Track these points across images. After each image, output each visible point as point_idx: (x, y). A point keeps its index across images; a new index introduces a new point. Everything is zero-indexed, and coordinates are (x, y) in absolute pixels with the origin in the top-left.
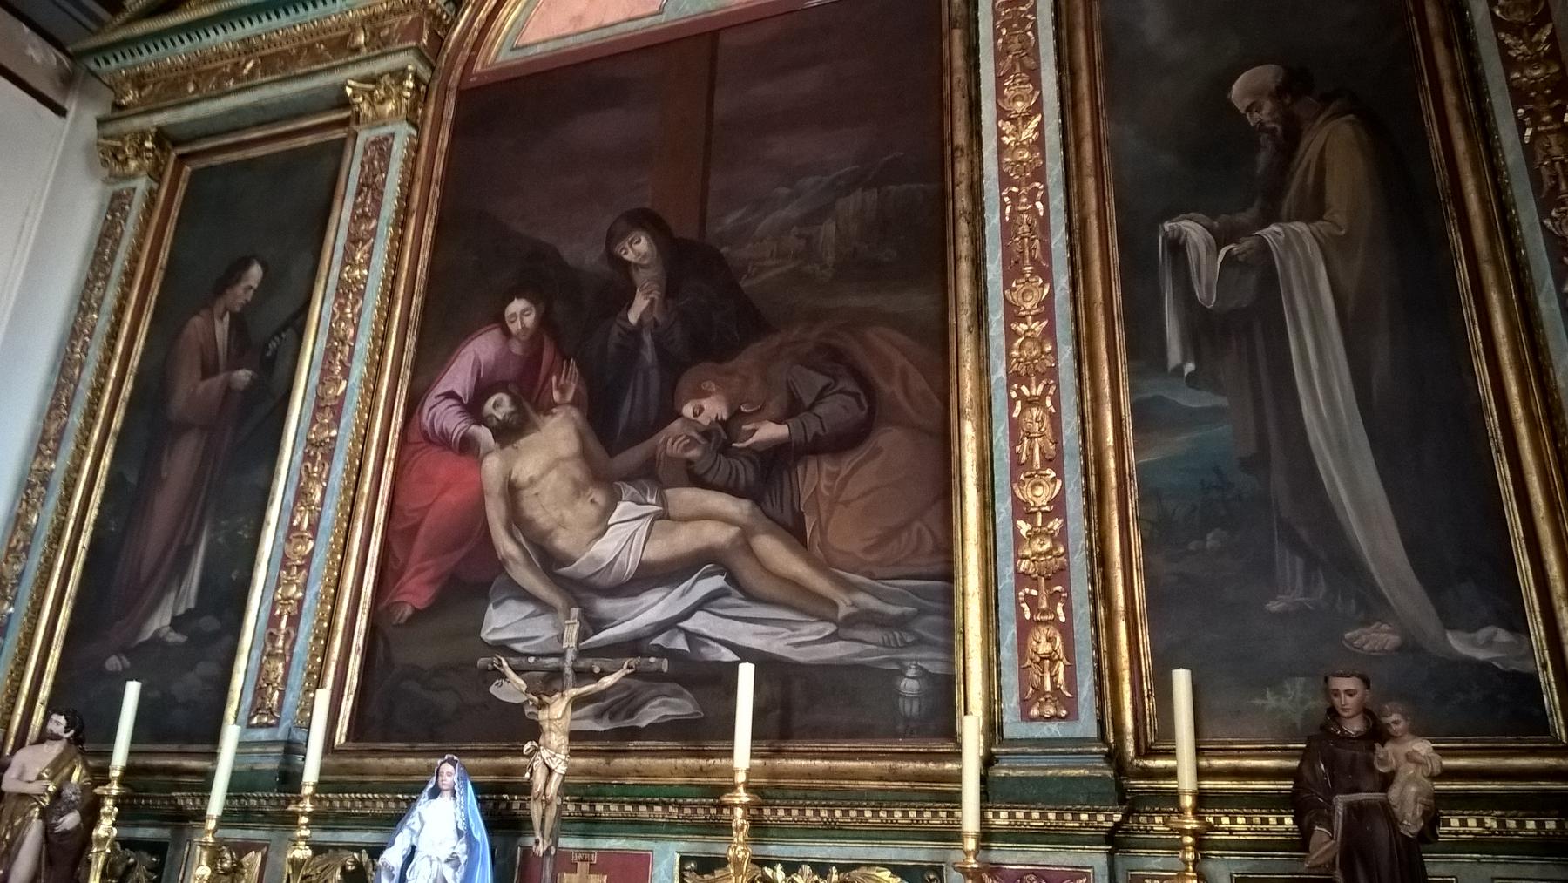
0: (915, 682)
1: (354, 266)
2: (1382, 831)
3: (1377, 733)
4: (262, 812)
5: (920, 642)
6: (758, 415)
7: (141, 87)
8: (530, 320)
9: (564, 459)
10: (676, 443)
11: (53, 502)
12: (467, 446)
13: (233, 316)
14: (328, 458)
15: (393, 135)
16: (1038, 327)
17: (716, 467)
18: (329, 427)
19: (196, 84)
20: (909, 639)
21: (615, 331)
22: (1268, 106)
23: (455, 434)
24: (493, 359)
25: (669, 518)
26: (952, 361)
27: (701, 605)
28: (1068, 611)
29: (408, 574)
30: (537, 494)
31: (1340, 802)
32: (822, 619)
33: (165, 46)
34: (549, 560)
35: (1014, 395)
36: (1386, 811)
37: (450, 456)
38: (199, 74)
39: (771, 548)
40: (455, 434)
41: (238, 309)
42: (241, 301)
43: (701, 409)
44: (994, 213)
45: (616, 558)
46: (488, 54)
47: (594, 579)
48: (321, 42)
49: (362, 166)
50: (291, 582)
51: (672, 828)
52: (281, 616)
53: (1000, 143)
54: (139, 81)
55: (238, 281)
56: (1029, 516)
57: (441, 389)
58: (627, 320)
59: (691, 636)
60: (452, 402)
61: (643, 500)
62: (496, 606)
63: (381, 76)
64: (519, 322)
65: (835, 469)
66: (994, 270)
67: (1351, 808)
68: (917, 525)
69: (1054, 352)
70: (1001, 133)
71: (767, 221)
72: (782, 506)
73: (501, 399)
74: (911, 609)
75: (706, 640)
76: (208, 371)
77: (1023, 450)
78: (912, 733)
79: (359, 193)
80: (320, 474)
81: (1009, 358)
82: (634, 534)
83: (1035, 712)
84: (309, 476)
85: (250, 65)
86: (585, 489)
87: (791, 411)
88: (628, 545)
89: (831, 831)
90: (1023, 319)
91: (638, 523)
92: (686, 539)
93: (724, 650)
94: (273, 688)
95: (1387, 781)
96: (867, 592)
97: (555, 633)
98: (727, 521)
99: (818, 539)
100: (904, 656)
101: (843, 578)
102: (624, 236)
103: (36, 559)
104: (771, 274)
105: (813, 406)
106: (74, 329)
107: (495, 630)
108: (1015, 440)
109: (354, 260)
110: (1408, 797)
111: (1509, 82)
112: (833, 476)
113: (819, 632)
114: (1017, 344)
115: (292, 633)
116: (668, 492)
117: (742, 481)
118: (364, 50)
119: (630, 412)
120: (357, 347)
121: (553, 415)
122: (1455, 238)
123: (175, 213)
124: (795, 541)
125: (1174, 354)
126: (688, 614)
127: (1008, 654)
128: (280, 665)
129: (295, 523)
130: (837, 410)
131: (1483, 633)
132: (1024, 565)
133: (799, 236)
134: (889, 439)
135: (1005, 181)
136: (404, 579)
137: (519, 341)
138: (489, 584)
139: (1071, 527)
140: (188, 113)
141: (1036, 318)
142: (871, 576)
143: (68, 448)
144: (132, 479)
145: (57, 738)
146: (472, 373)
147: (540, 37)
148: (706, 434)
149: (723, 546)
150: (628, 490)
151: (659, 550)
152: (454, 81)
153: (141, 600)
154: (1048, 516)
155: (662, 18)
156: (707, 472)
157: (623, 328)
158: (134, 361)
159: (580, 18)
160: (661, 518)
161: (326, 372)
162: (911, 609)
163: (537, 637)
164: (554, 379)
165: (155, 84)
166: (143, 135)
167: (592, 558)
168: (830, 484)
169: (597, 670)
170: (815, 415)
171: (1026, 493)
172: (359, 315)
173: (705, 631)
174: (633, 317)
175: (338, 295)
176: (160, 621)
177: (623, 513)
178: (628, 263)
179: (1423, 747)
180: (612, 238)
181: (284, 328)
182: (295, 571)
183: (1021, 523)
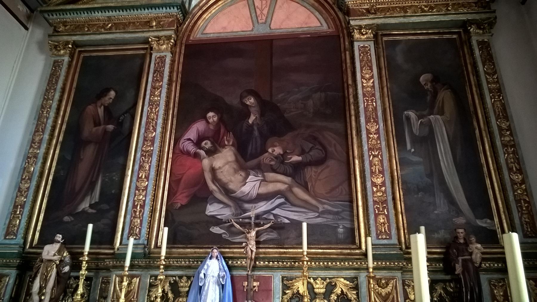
0: (342, 230)
1: (155, 96)
2: (470, 265)
4: (138, 266)
5: (343, 219)
6: (292, 153)
7: (65, 26)
8: (216, 119)
9: (230, 162)
10: (267, 160)
11: (39, 164)
12: (196, 155)
13: (105, 107)
14: (151, 156)
15: (166, 56)
16: (376, 136)
17: (280, 167)
18: (150, 146)
19: (87, 28)
20: (340, 218)
21: (245, 125)
22: (429, 84)
23: (192, 152)
24: (203, 129)
25: (266, 181)
26: (350, 143)
27: (277, 207)
28: (388, 211)
29: (178, 194)
30: (222, 172)
31: (460, 259)
32: (315, 211)
33: (77, 14)
34: (227, 192)
35: (370, 154)
36: (471, 260)
37: (191, 158)
38: (89, 25)
39: (298, 191)
40: (192, 152)
41: (106, 105)
42: (108, 102)
43: (274, 151)
44: (362, 104)
45: (249, 192)
46: (194, 35)
47: (243, 198)
48: (137, 22)
49: (155, 64)
50: (140, 195)
51: (279, 268)
52: (137, 205)
53: (362, 85)
54: (65, 24)
55: (106, 96)
56: (376, 186)
57: (186, 137)
58: (249, 122)
59: (275, 215)
60: (190, 142)
61: (257, 175)
62: (210, 205)
63: (162, 37)
64: (212, 119)
65: (316, 170)
66: (363, 120)
67: (463, 260)
68: (340, 187)
69: (380, 143)
70: (362, 83)
71: (292, 98)
72: (301, 179)
73: (207, 142)
74: (340, 210)
75: (281, 217)
76: (97, 124)
77: (373, 168)
78: (342, 243)
79: (154, 73)
80: (148, 161)
81: (368, 144)
82: (255, 185)
83: (380, 237)
84: (144, 161)
85: (110, 25)
86: (238, 171)
87: (302, 153)
88: (253, 188)
89: (327, 268)
90: (371, 134)
91: (257, 182)
92: (271, 188)
93: (285, 219)
94: (137, 228)
95: (471, 254)
96: (327, 204)
97: (231, 213)
98: (285, 183)
99: (312, 189)
100: (339, 222)
101: (320, 200)
102: (246, 97)
103: (34, 183)
104: (294, 113)
105: (308, 152)
106: (42, 105)
107: (210, 212)
108: (371, 166)
109: (155, 94)
111: (488, 87)
112: (315, 172)
113: (314, 215)
114: (370, 140)
115: (143, 211)
116: (265, 174)
117: (288, 172)
118: (155, 27)
119: (252, 150)
120: (158, 122)
121: (226, 148)
122: (475, 124)
123: (78, 70)
124: (305, 189)
125: (409, 146)
126: (274, 209)
127: (372, 222)
128: (139, 221)
129: (140, 176)
130: (315, 154)
131: (484, 220)
132: (375, 199)
133: (302, 103)
134: (331, 163)
135: (364, 95)
136: (177, 195)
137: (212, 125)
138: (207, 198)
139: (387, 189)
140: (86, 38)
141: (375, 134)
142: (328, 200)
143: (44, 146)
144: (69, 157)
145: (59, 242)
146: (197, 134)
147: (211, 32)
148: (276, 157)
149: (284, 190)
150: (252, 172)
151: (263, 190)
152: (184, 42)
154: (381, 187)
155: (253, 33)
156: (277, 169)
157: (247, 124)
158: (66, 119)
159: (225, 28)
160: (263, 181)
161: (147, 129)
162: (340, 210)
163: (225, 214)
164: (225, 137)
165: (71, 25)
166: (67, 43)
167: (241, 192)
168: (315, 174)
169: (262, 223)
170: (310, 155)
171: (375, 180)
172: (158, 111)
173: (279, 214)
174: (250, 121)
175: (149, 105)
177: (250, 179)
178: (247, 105)
179: (479, 246)
180: (242, 97)
181: (126, 112)
182: (141, 191)
183: (374, 188)
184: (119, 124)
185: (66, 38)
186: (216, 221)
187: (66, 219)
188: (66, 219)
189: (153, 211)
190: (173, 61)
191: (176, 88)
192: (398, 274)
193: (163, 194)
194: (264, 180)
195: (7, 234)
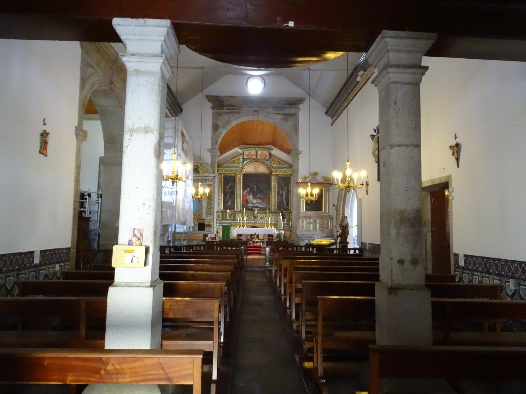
3: (283, 211)
34: (252, 202)
39: (262, 202)
92: (258, 202)
103: (221, 200)
110: (284, 213)
153: (228, 202)
161: (238, 191)
176: (229, 204)
184: (233, 190)
185: (221, 173)
186: (249, 206)
189: (240, 205)
191: (242, 184)
192: (275, 215)
193: (242, 202)
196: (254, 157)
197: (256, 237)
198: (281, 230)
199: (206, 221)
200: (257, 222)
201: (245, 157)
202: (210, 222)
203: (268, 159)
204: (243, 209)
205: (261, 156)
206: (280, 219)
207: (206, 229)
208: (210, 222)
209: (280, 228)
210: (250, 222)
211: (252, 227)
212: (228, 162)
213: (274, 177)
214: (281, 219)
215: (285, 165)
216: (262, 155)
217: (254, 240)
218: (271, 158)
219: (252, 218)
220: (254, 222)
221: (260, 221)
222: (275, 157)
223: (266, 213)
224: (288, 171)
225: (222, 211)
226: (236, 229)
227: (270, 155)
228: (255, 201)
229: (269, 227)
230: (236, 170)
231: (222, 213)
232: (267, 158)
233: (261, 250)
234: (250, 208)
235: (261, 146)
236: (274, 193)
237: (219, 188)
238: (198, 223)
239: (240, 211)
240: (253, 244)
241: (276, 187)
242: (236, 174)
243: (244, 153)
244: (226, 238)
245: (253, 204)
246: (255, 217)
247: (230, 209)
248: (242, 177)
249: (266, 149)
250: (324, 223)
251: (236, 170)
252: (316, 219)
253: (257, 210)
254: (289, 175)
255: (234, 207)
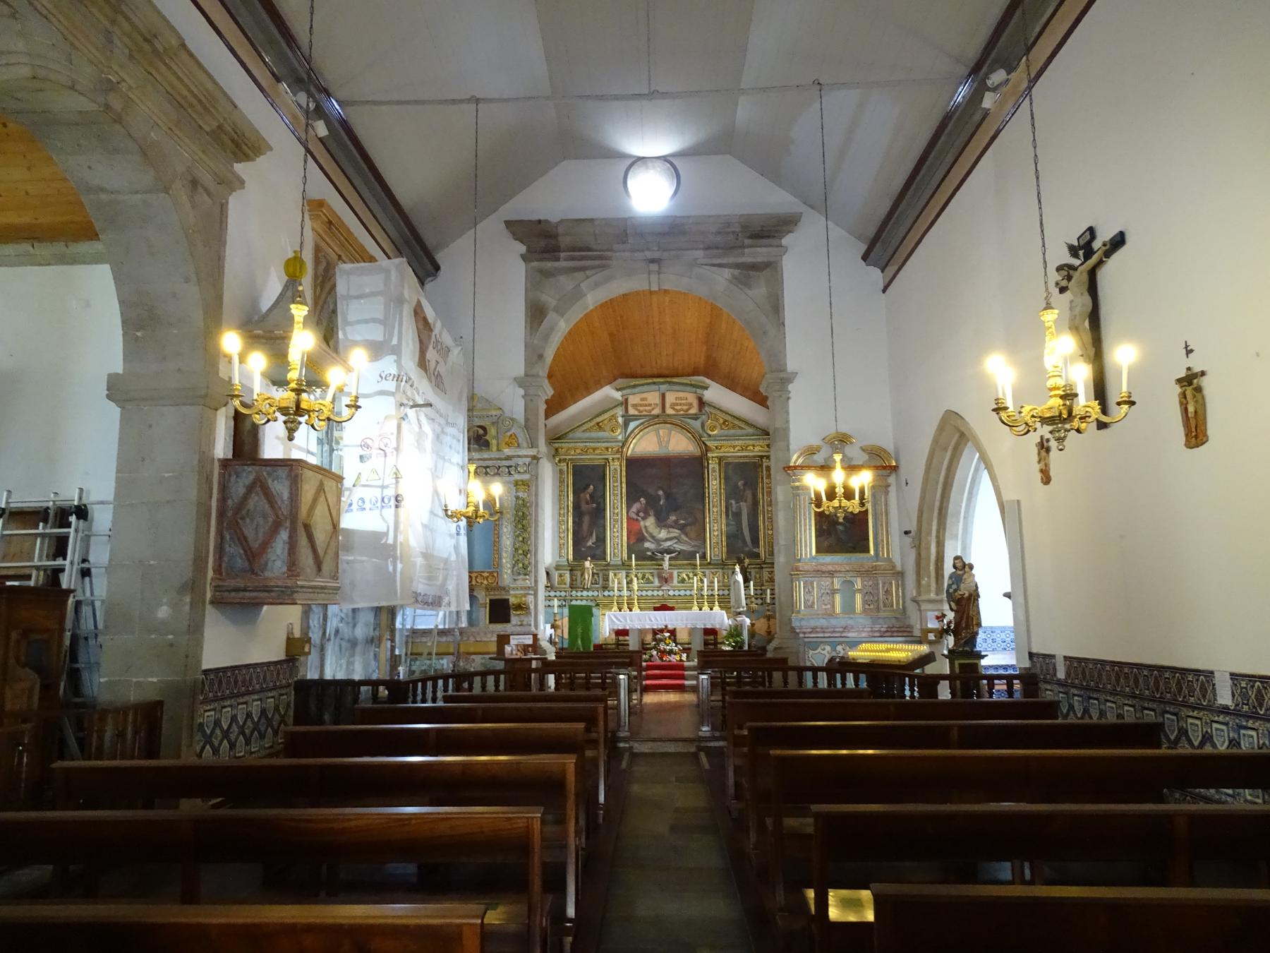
12: (637, 520)
34: (653, 537)
39: (683, 537)
92: (672, 535)
110: (746, 565)
144: (577, 520)
151: (668, 536)
153: (585, 539)
161: (614, 508)
176: (590, 543)
184: (598, 504)
186: (648, 549)
187: (583, 549)
188: (583, 549)
189: (622, 546)
190: (621, 471)
191: (624, 485)
192: (720, 570)
193: (625, 538)
194: (669, 532)
195: (560, 556)
196: (657, 411)
197: (670, 638)
198: (740, 613)
199: (512, 592)
200: (671, 593)
201: (632, 411)
202: (525, 597)
203: (696, 414)
204: (630, 558)
205: (676, 407)
206: (736, 582)
207: (514, 620)
208: (525, 595)
209: (738, 610)
210: (650, 593)
211: (656, 609)
212: (584, 427)
213: (713, 465)
214: (738, 582)
215: (742, 428)
216: (677, 405)
217: (662, 646)
218: (704, 411)
219: (657, 583)
220: (660, 593)
221: (679, 591)
222: (715, 407)
223: (696, 565)
224: (754, 446)
225: (569, 565)
226: (609, 615)
227: (702, 403)
228: (663, 534)
229: (706, 608)
230: (607, 449)
231: (571, 570)
232: (693, 411)
233: (683, 677)
234: (649, 553)
235: (675, 380)
236: (715, 510)
237: (560, 500)
238: (488, 601)
239: (620, 563)
240: (661, 658)
241: (720, 493)
242: (607, 459)
243: (627, 400)
244: (580, 642)
245: (658, 541)
246: (665, 580)
247: (594, 558)
248: (624, 469)
249: (689, 388)
250: (878, 589)
251: (607, 449)
252: (852, 579)
253: (671, 559)
254: (754, 457)
255: (604, 553)
